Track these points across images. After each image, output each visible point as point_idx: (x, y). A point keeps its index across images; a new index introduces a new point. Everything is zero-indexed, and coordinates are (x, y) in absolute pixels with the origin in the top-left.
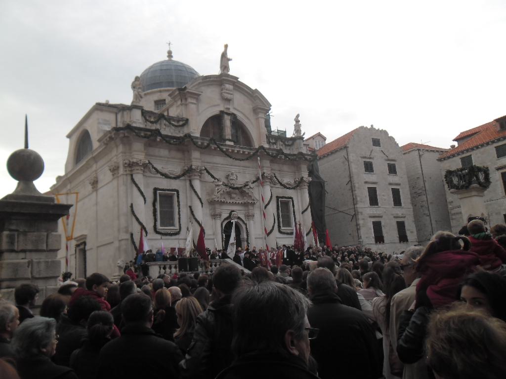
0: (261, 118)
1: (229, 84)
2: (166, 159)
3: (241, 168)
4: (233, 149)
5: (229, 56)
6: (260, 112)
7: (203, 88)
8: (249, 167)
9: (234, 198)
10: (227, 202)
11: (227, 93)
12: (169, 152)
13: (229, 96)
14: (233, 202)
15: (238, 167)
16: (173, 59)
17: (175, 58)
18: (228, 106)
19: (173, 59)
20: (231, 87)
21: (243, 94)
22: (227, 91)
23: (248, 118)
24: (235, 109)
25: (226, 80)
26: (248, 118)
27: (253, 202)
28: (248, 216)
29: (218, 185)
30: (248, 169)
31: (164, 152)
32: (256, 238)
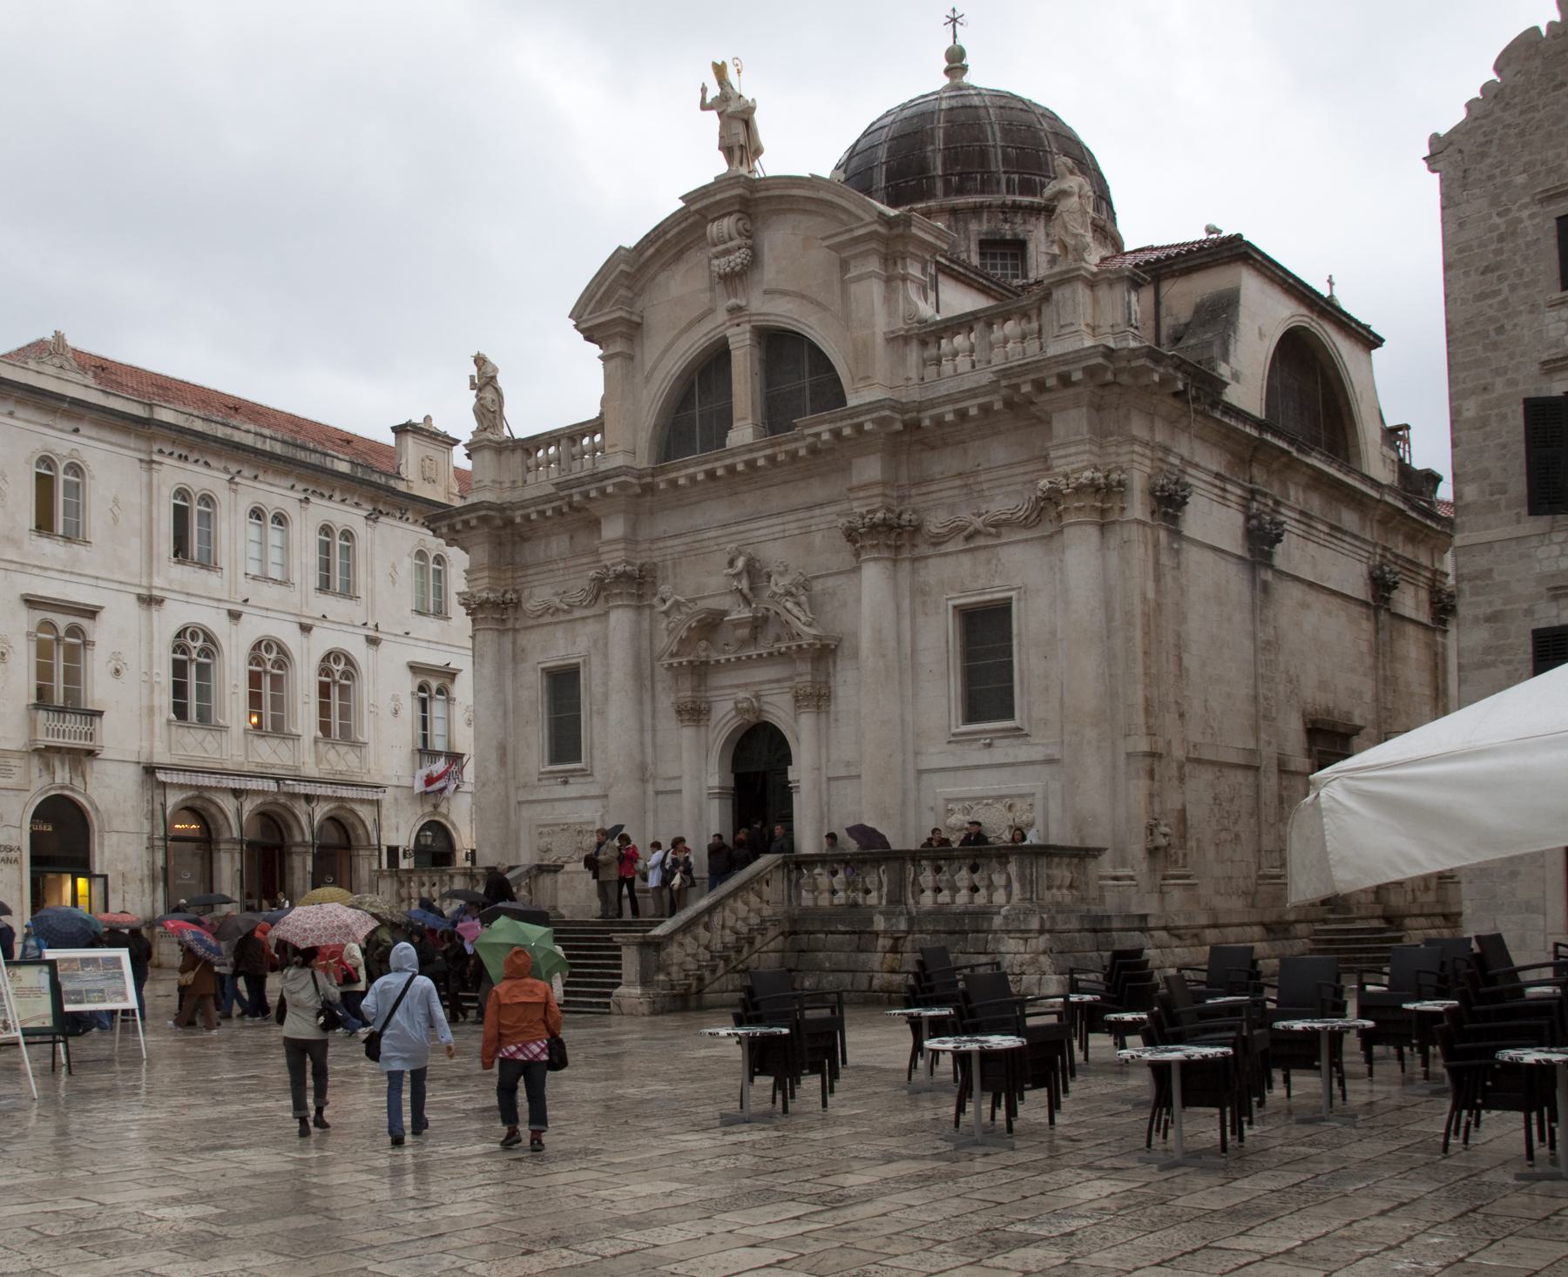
0: (859, 278)
1: (718, 218)
2: (561, 565)
3: (786, 519)
4: (728, 462)
5: (746, 86)
6: (854, 257)
7: (661, 278)
8: (821, 505)
9: (744, 643)
10: (718, 662)
11: (727, 252)
12: (572, 537)
13: (721, 265)
14: (739, 659)
15: (780, 520)
16: (968, 79)
17: (980, 76)
18: (733, 302)
19: (968, 79)
20: (727, 225)
21: (805, 211)
22: (721, 248)
23: (818, 304)
24: (766, 292)
25: (706, 208)
26: (818, 304)
27: (794, 645)
28: (820, 697)
29: (667, 613)
30: (817, 512)
31: (558, 545)
32: (829, 779)
